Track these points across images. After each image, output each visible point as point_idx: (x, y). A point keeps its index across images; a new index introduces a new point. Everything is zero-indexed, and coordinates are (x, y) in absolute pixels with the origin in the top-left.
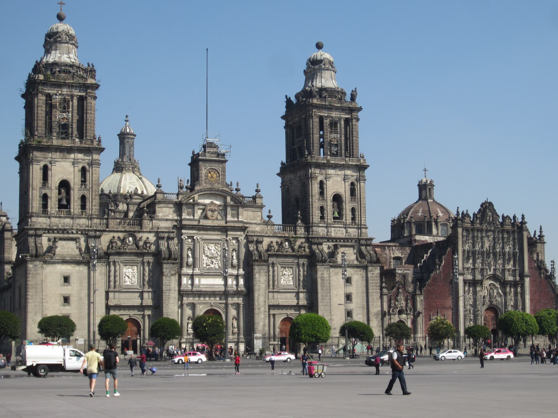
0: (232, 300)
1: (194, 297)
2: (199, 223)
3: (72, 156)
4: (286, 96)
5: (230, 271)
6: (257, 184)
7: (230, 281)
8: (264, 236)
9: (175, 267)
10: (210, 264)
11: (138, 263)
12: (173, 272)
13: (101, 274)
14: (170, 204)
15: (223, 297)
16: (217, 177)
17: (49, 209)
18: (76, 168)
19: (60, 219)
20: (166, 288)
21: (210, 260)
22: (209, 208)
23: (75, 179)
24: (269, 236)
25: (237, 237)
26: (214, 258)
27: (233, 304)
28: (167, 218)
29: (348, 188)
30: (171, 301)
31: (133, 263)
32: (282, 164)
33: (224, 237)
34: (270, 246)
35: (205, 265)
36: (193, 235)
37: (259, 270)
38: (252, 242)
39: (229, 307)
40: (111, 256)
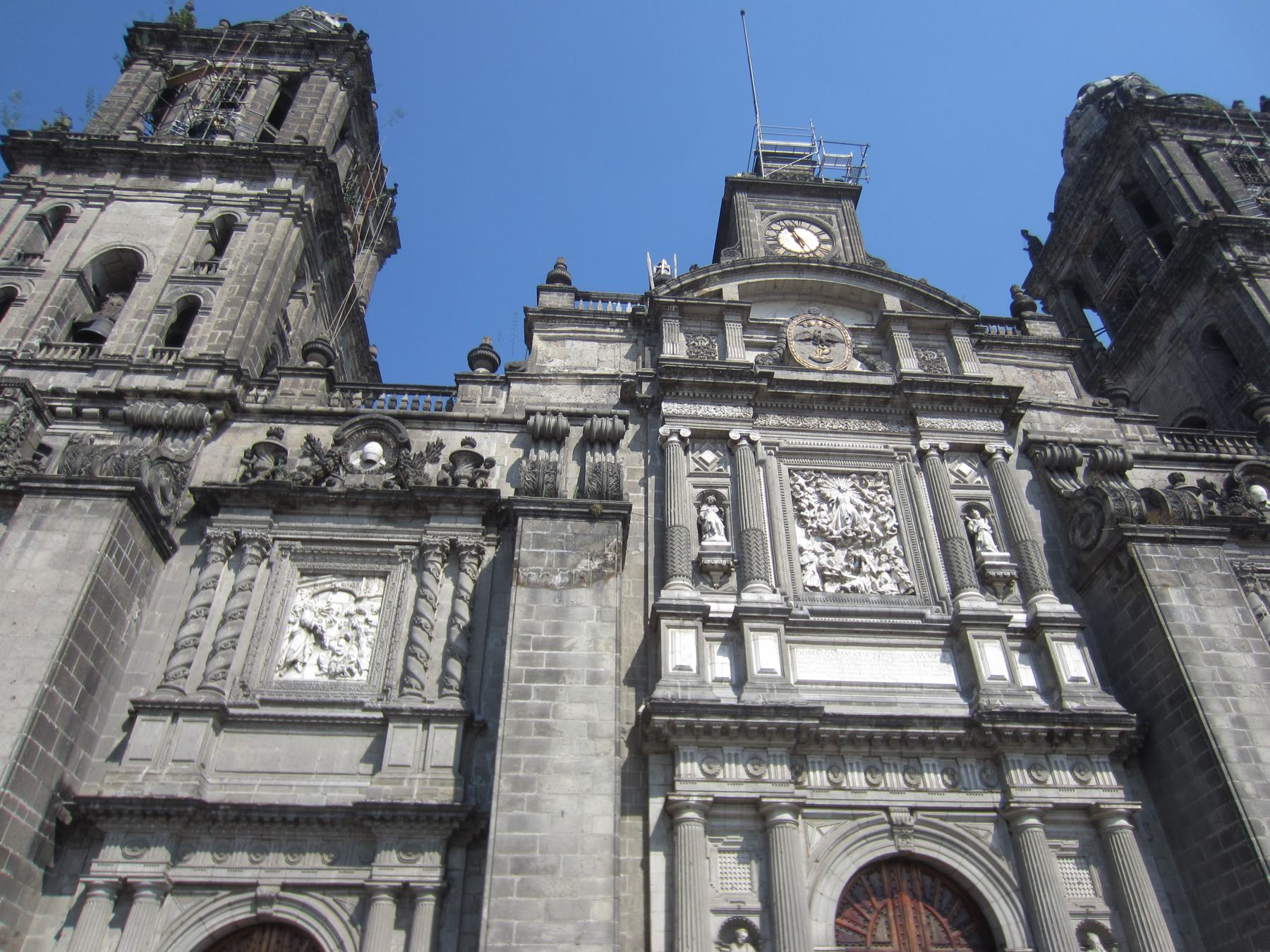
0: (1041, 784)
1: (756, 760)
4: (1024, 233)
5: (974, 601)
9: (598, 538)
10: (846, 574)
11: (392, 560)
12: (585, 565)
14: (605, 324)
15: (970, 770)
20: (525, 659)
21: (840, 555)
25: (975, 440)
26: (866, 546)
27: (1052, 815)
30: (563, 754)
31: (364, 558)
33: (906, 443)
35: (814, 580)
36: (722, 426)
37: (1177, 565)
39: (1024, 838)
40: (229, 509)
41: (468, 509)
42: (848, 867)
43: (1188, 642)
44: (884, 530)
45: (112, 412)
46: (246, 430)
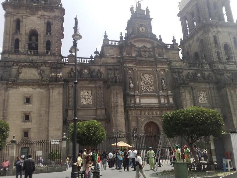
2: (136, 59)
3: (40, 13)
5: (161, 92)
6: (174, 37)
7: (162, 100)
8: (182, 69)
13: (59, 94)
16: (146, 30)
17: (20, 49)
18: (43, 22)
19: (29, 56)
20: (114, 104)
22: (142, 49)
23: (41, 29)
24: (186, 69)
28: (113, 56)
29: (232, 40)
30: (119, 114)
32: (181, 39)
34: (187, 76)
35: (143, 89)
36: (132, 68)
38: (175, 72)
41: (101, 81)
42: (145, 123)
43: (183, 100)
44: (151, 82)
45: (47, 65)
46: (67, 67)
